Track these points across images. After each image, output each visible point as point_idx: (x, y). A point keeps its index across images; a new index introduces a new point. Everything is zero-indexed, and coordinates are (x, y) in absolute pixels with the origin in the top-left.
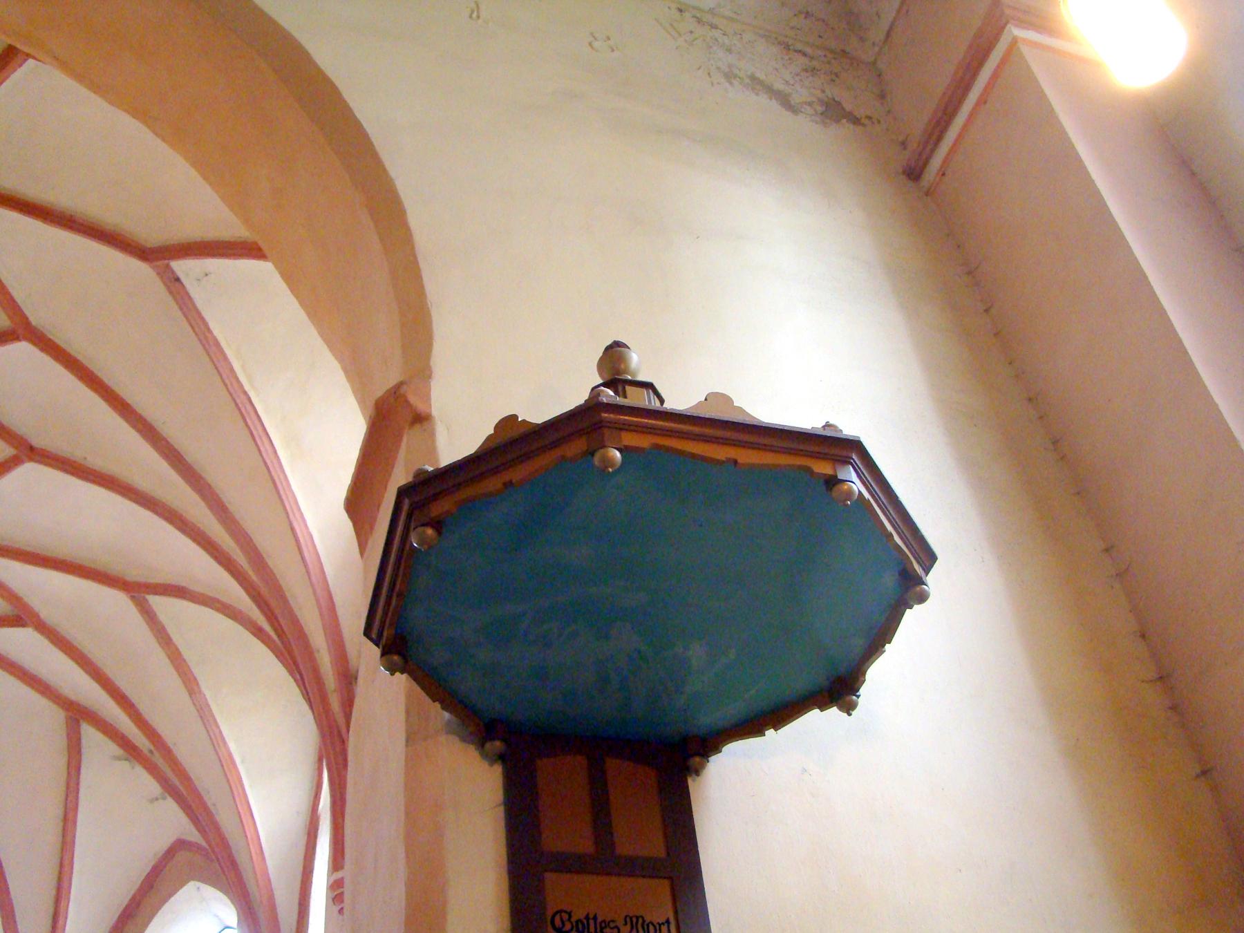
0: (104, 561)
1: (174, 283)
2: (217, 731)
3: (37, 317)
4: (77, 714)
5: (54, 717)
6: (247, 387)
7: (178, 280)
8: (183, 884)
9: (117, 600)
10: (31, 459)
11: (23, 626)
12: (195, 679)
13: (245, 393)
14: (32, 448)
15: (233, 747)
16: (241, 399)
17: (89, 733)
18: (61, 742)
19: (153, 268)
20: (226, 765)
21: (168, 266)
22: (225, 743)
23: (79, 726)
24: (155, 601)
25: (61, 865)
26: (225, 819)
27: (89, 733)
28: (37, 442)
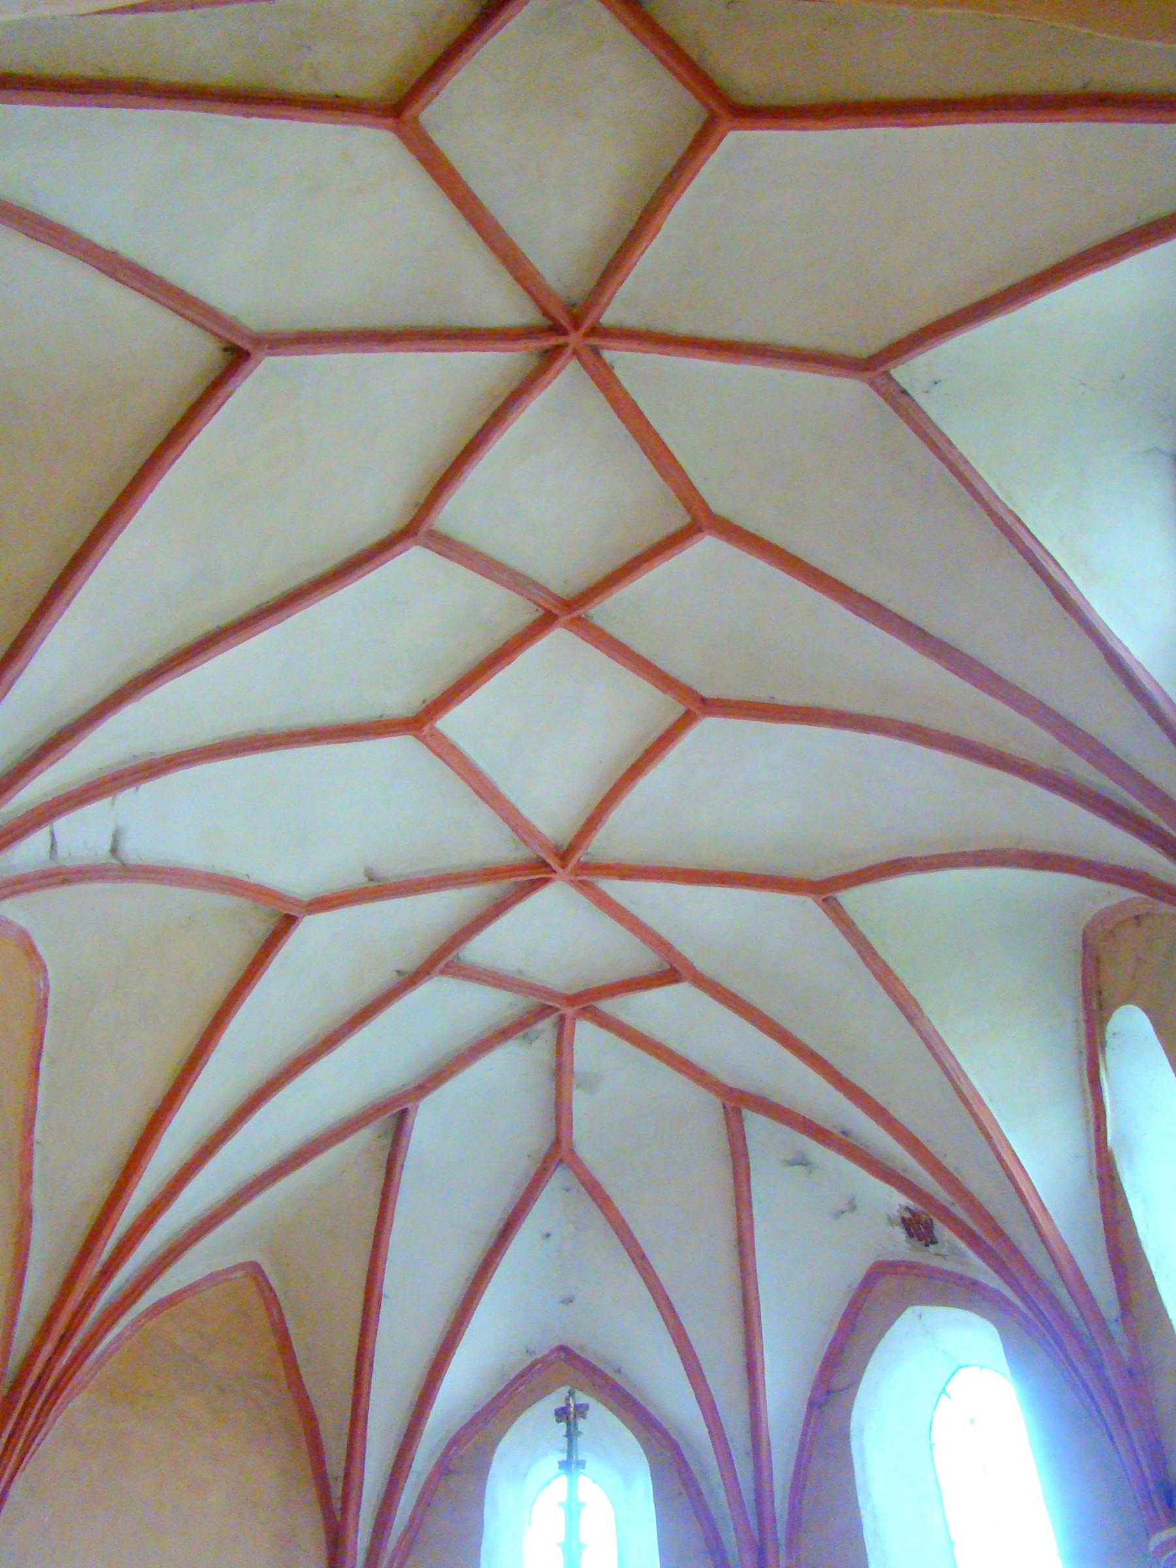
1: (900, 401)
2: (952, 1062)
4: (737, 1102)
6: (1011, 507)
7: (904, 392)
8: (899, 1312)
11: (676, 981)
12: (914, 1000)
13: (1012, 512)
16: (1009, 520)
17: (756, 1125)
18: (719, 1143)
22: (966, 1077)
23: (740, 1120)
25: (745, 1301)
26: (982, 1184)
27: (756, 1125)
28: (707, 692)
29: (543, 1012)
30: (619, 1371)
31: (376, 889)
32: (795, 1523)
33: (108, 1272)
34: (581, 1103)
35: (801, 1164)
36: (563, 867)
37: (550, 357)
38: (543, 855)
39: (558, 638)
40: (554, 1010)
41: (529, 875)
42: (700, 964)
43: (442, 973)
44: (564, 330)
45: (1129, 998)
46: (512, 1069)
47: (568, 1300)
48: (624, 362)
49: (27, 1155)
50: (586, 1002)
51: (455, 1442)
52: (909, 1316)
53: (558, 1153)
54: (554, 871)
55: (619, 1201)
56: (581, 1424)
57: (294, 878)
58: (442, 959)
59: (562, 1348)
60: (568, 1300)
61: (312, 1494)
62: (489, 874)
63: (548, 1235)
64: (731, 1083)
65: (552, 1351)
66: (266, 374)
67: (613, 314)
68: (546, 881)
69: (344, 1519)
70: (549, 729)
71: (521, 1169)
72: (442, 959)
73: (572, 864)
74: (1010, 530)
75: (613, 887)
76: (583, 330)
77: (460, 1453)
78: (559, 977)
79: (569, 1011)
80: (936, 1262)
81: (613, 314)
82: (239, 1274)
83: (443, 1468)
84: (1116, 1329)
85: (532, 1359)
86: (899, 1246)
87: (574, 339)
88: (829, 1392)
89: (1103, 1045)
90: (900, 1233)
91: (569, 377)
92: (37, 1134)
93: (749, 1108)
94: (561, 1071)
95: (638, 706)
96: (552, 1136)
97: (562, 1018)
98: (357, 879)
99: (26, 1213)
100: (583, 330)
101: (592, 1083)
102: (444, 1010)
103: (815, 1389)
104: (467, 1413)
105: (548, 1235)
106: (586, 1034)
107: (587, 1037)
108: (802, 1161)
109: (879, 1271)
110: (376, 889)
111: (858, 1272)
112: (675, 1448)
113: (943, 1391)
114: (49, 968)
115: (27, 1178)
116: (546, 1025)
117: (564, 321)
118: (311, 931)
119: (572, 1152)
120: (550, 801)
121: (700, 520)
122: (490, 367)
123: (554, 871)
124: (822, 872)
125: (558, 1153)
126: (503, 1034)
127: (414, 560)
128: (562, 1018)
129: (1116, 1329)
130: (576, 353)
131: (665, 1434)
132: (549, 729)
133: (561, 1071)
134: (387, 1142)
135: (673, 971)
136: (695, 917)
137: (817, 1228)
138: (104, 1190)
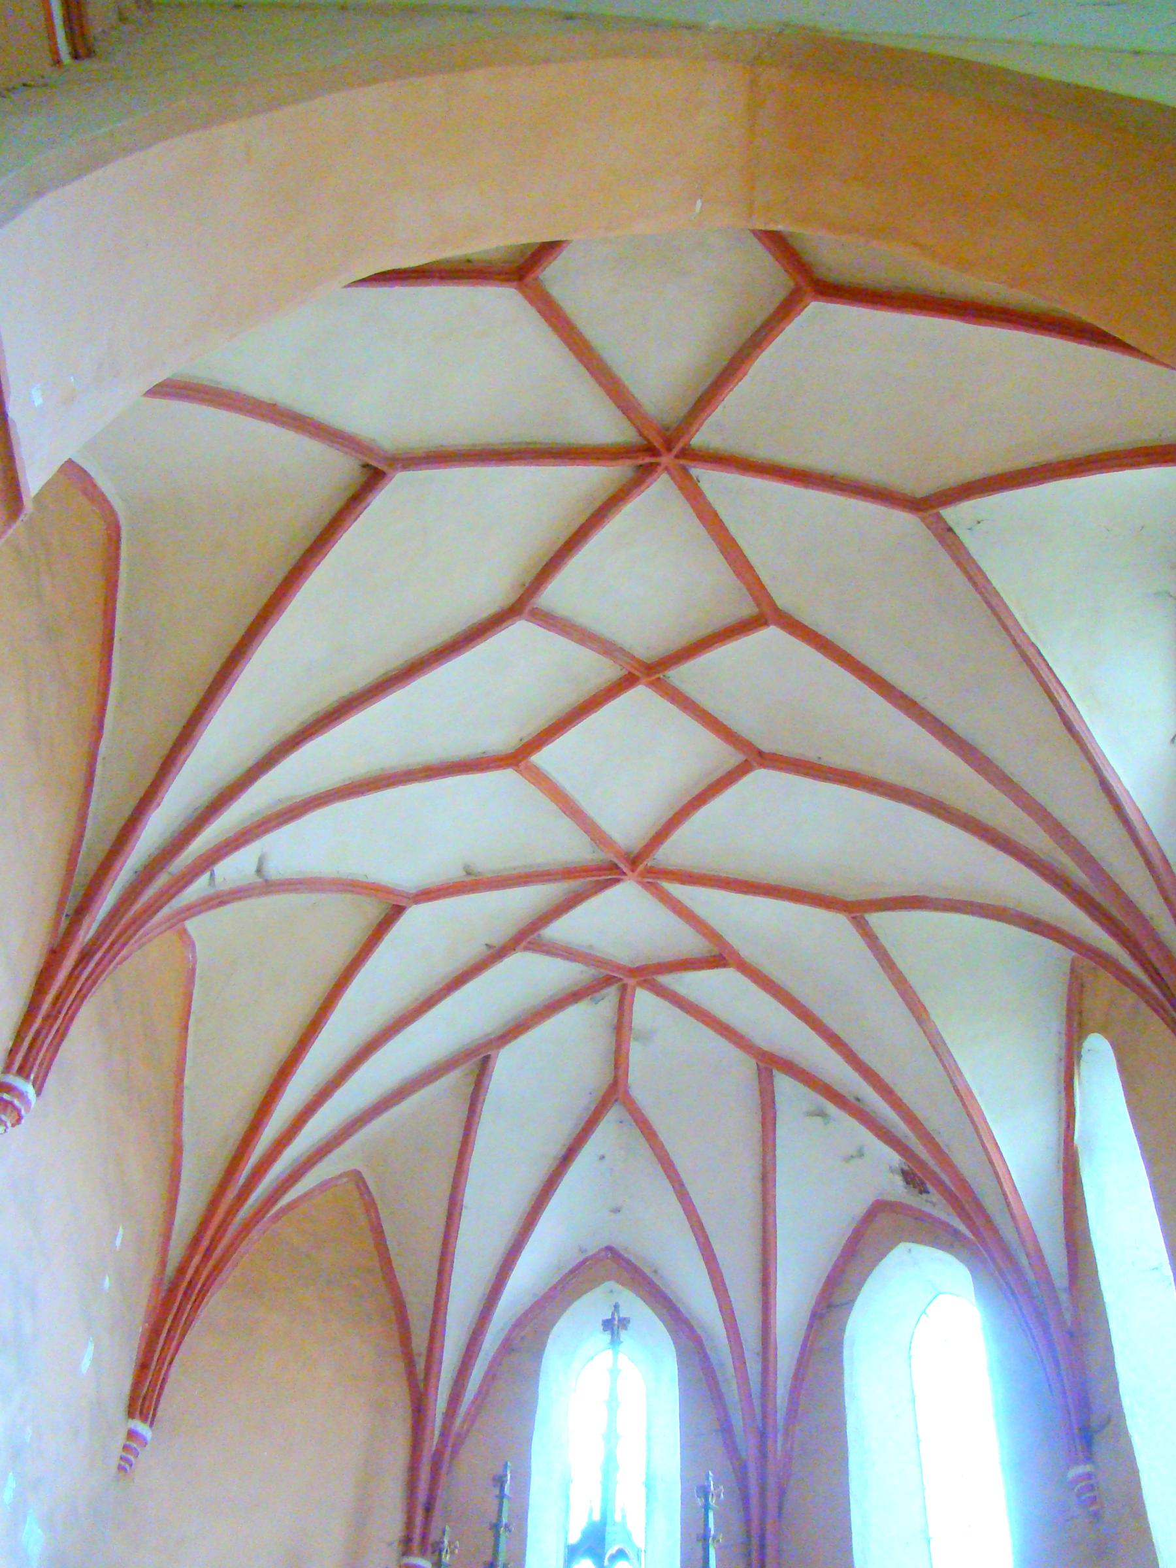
0: (817, 882)
1: (946, 535)
2: (951, 1061)
3: (783, 598)
4: (770, 1064)
5: (743, 1067)
6: (1033, 639)
7: (950, 529)
8: (895, 1244)
9: (841, 921)
10: (762, 766)
11: (725, 965)
13: (1033, 645)
14: (760, 753)
15: (968, 1077)
16: (1030, 652)
19: (923, 520)
20: (963, 1097)
21: (938, 516)
23: (771, 1076)
24: (877, 920)
26: (966, 1160)
27: (783, 1083)
28: (766, 747)
29: (608, 981)
30: (656, 1272)
31: (472, 883)
32: (793, 1412)
33: (243, 1196)
34: (636, 1053)
35: (818, 1115)
36: (633, 871)
37: (644, 474)
38: (616, 860)
39: (640, 693)
40: (615, 980)
41: (602, 874)
42: (747, 952)
43: (527, 949)
44: (658, 450)
45: (1104, 1031)
46: (580, 1028)
47: (617, 1210)
48: (709, 479)
49: (178, 1102)
50: (648, 974)
51: (519, 1324)
52: (902, 1247)
53: (615, 1092)
54: (624, 874)
55: (663, 1135)
56: (624, 1335)
57: (402, 874)
58: (527, 937)
59: (609, 1249)
60: (617, 1210)
61: (400, 1366)
62: (569, 873)
63: (602, 1157)
64: (765, 1047)
65: (602, 1250)
66: (399, 487)
67: (704, 437)
68: (617, 881)
69: (426, 1388)
70: (629, 764)
71: (580, 1104)
72: (527, 937)
73: (641, 867)
74: (1031, 661)
75: (675, 889)
76: (675, 451)
77: (523, 1334)
78: (623, 955)
79: (631, 982)
80: (927, 1208)
81: (704, 437)
82: (345, 1180)
83: (507, 1347)
84: (1064, 1297)
85: (585, 1256)
86: (897, 1189)
87: (666, 460)
88: (829, 1306)
89: (1080, 1057)
90: (899, 1180)
91: (661, 487)
92: (186, 1082)
93: (778, 1069)
94: (621, 1027)
95: (706, 753)
96: (609, 1078)
97: (624, 988)
98: (454, 873)
99: (178, 1147)
100: (675, 451)
101: (646, 1037)
102: (527, 976)
103: (818, 1303)
104: (528, 1301)
105: (602, 1157)
106: (644, 1002)
107: (644, 1002)
108: (821, 1113)
109: (879, 1208)
110: (472, 883)
111: (860, 1207)
112: (698, 1341)
113: (924, 1312)
114: (197, 944)
115: (179, 1117)
116: (611, 994)
117: (658, 443)
118: (416, 916)
119: (627, 1093)
120: (625, 819)
121: (765, 614)
122: (590, 480)
123: (624, 874)
124: (853, 894)
125: (615, 1092)
126: (574, 996)
127: (520, 630)
128: (624, 988)
129: (1064, 1297)
130: (667, 469)
131: (692, 1329)
132: (629, 764)
133: (621, 1027)
134: (472, 1080)
135: (720, 956)
136: (740, 917)
137: (827, 1173)
138: (239, 1129)
